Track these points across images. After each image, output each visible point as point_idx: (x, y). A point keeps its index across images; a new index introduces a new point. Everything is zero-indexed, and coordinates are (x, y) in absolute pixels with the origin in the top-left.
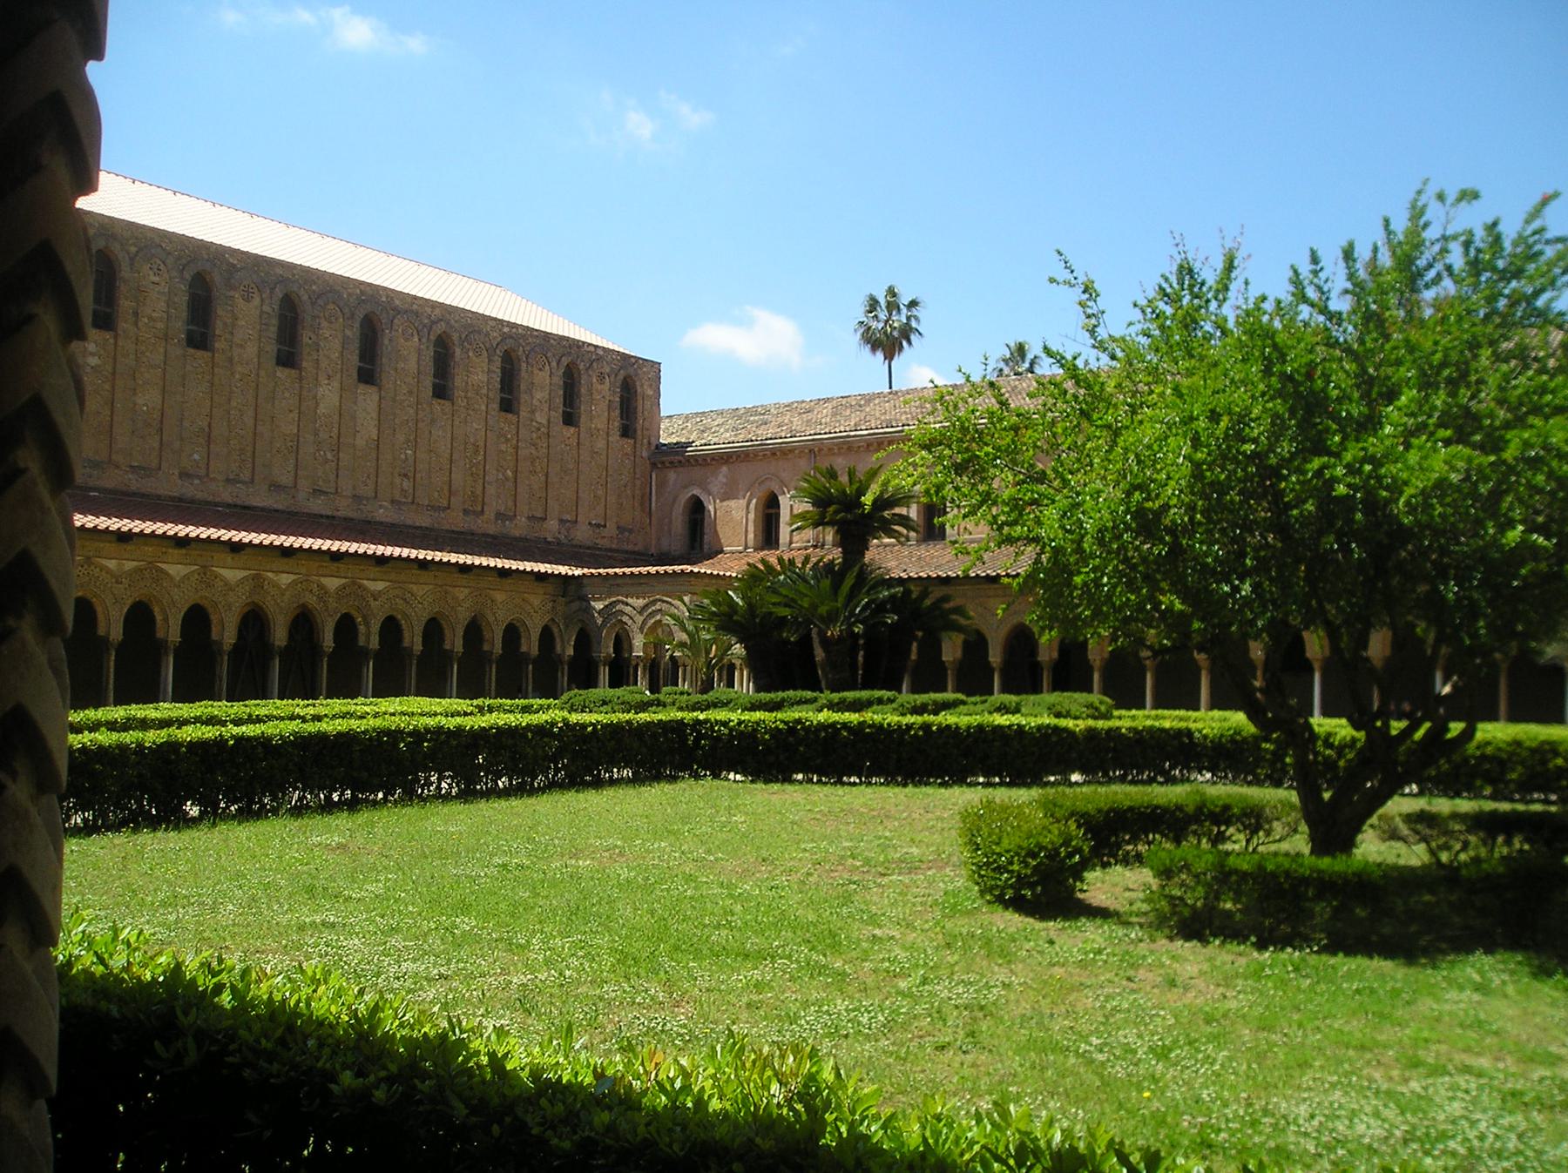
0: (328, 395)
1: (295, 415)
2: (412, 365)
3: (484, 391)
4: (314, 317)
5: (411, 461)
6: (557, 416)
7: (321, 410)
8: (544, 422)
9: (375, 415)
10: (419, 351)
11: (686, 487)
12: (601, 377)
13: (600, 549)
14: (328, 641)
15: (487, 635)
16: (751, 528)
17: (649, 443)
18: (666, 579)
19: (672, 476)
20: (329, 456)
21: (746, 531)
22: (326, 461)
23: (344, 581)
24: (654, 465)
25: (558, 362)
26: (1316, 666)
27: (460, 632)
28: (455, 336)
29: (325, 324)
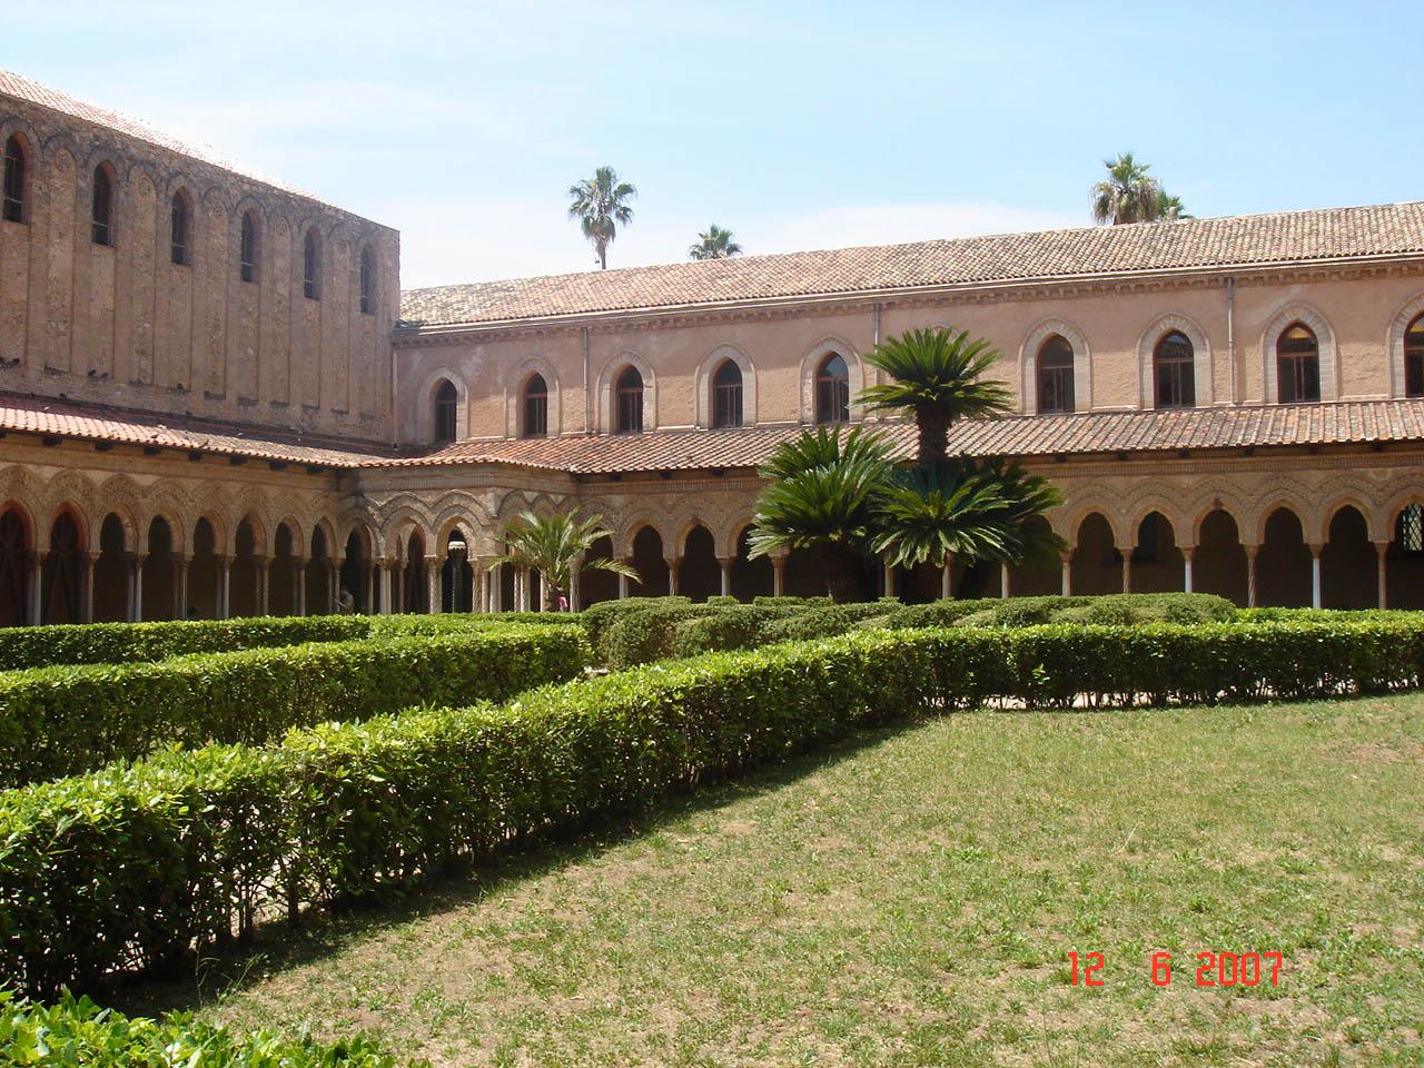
0: (61, 255)
1: (24, 278)
2: (149, 224)
3: (224, 257)
4: (45, 163)
5: (149, 336)
6: (299, 287)
7: (53, 274)
8: (286, 294)
9: (110, 281)
10: (157, 209)
11: (433, 369)
12: (342, 245)
13: (343, 439)
14: (94, 547)
15: (258, 536)
16: (513, 415)
17: (390, 320)
18: (465, 470)
19: (417, 357)
20: (62, 328)
21: (507, 418)
22: (59, 334)
23: (110, 474)
24: (394, 345)
25: (299, 227)
26: (1187, 556)
27: (233, 535)
28: (194, 192)
29: (56, 172)
